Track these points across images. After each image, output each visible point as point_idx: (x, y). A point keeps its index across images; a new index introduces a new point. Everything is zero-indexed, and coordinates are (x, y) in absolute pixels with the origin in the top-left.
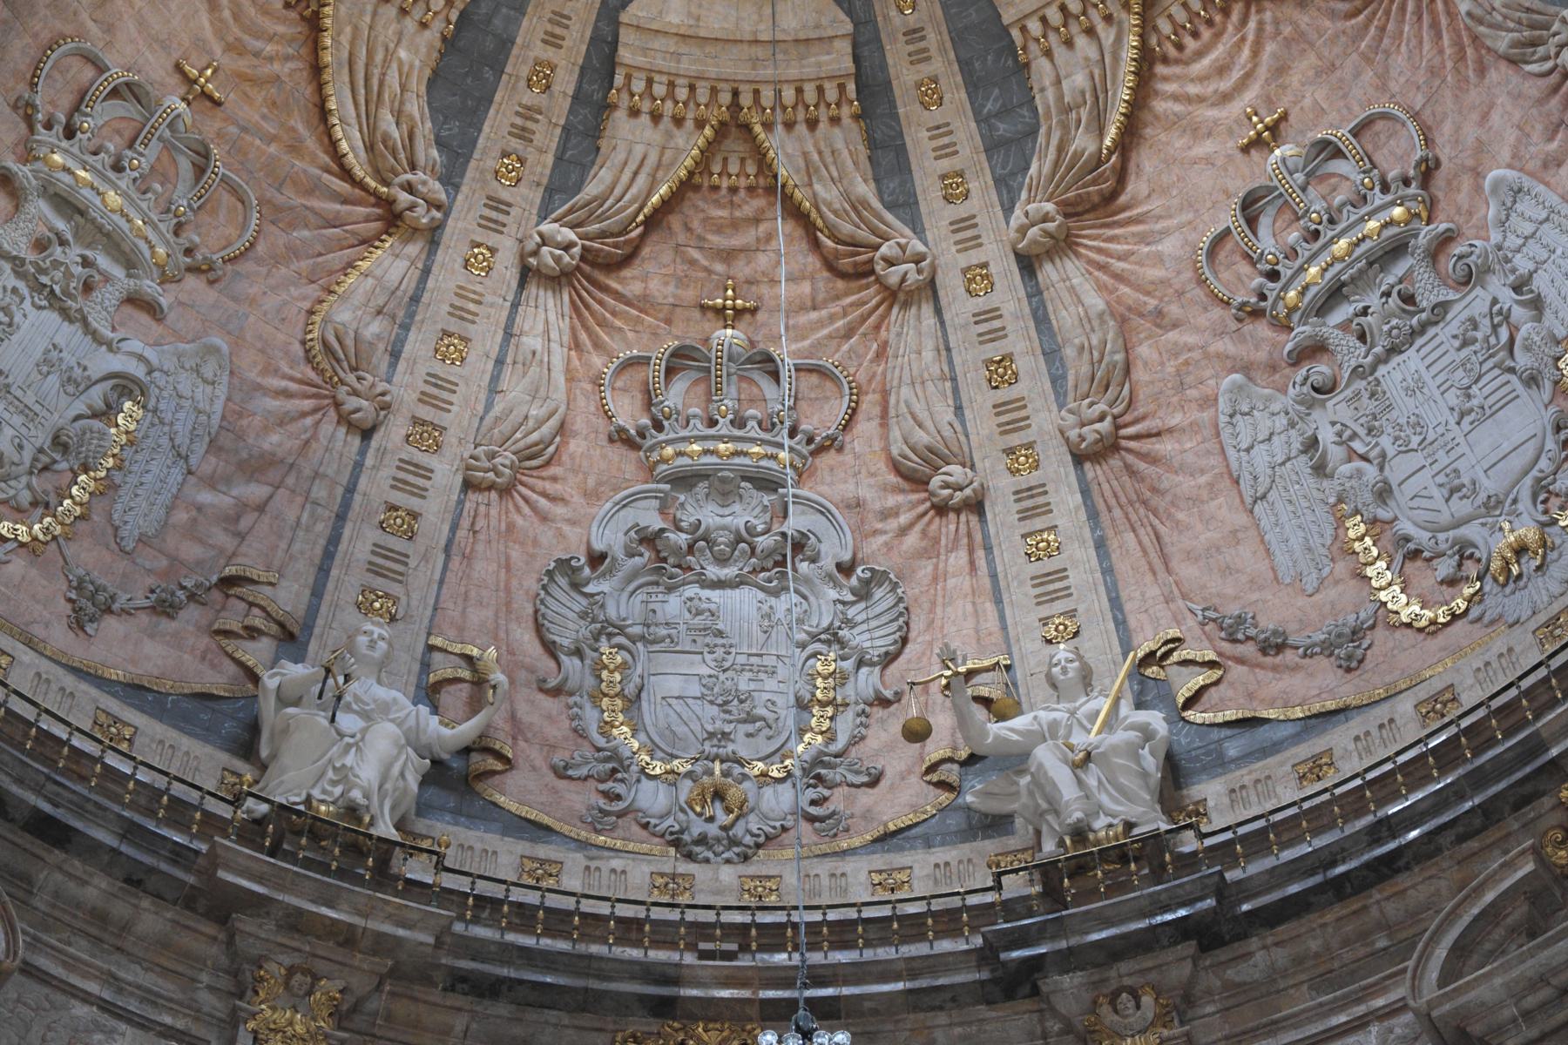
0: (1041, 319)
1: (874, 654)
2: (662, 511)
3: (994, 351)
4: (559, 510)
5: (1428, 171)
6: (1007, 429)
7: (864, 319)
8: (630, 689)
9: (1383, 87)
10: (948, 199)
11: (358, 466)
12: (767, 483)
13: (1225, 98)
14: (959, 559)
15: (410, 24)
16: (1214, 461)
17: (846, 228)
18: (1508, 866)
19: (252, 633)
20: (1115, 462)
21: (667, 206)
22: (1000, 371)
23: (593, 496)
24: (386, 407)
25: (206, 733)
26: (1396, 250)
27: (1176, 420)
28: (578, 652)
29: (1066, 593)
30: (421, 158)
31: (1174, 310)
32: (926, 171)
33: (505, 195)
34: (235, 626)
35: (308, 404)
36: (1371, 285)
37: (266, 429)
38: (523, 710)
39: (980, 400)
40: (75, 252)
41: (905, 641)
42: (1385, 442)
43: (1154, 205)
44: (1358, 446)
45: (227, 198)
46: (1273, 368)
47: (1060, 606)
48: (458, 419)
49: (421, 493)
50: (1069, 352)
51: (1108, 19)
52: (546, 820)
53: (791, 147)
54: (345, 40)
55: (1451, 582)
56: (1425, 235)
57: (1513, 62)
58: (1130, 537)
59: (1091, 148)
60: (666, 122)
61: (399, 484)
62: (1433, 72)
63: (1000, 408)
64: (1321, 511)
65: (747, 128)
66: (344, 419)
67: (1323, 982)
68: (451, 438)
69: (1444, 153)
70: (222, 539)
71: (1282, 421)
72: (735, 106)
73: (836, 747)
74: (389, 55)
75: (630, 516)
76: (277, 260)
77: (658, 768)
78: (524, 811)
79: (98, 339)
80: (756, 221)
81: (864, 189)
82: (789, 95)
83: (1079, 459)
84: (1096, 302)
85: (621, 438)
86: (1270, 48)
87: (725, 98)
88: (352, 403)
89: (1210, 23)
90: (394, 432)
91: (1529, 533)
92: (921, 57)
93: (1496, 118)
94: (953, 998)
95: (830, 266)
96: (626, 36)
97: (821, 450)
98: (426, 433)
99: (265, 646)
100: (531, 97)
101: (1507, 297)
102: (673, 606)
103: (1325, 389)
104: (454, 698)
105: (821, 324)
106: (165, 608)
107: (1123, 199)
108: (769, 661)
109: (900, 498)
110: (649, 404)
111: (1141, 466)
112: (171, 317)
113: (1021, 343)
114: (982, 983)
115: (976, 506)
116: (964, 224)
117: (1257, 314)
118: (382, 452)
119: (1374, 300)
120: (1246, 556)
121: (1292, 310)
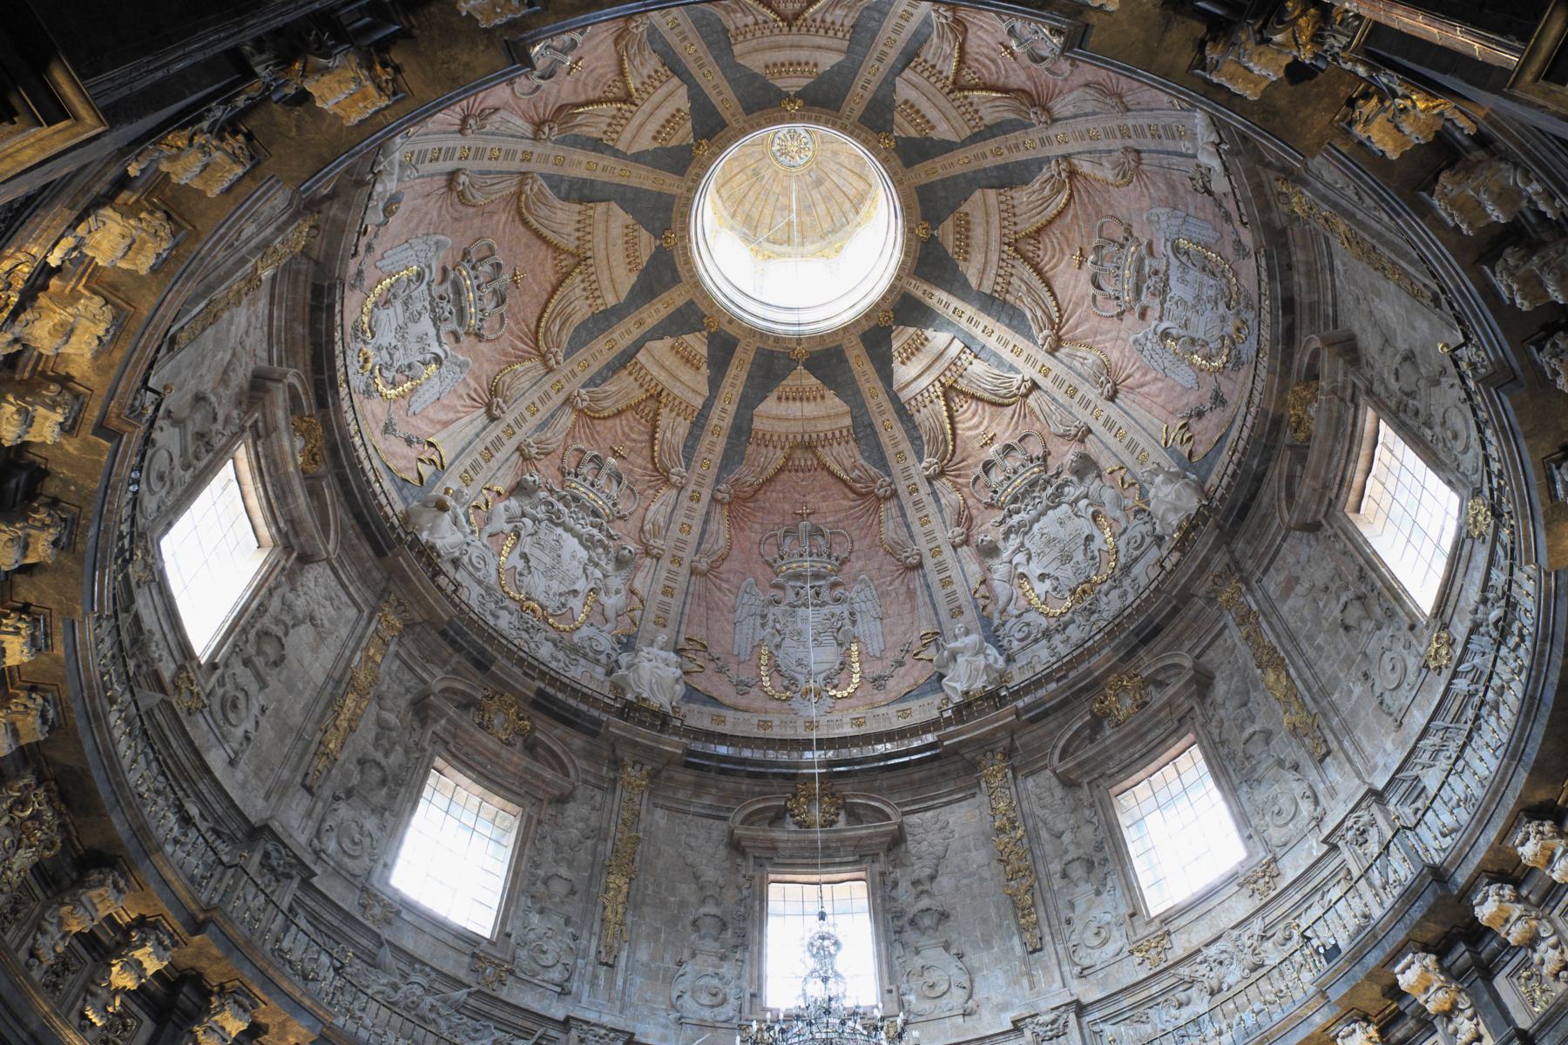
11: (1150, 151)
21: (997, 91)
45: (1105, 234)
53: (945, 68)
65: (954, 83)
72: (951, 91)
76: (1111, 206)
82: (933, 79)
88: (1133, 164)
90: (1131, 143)
95: (966, 30)
96: (963, 136)
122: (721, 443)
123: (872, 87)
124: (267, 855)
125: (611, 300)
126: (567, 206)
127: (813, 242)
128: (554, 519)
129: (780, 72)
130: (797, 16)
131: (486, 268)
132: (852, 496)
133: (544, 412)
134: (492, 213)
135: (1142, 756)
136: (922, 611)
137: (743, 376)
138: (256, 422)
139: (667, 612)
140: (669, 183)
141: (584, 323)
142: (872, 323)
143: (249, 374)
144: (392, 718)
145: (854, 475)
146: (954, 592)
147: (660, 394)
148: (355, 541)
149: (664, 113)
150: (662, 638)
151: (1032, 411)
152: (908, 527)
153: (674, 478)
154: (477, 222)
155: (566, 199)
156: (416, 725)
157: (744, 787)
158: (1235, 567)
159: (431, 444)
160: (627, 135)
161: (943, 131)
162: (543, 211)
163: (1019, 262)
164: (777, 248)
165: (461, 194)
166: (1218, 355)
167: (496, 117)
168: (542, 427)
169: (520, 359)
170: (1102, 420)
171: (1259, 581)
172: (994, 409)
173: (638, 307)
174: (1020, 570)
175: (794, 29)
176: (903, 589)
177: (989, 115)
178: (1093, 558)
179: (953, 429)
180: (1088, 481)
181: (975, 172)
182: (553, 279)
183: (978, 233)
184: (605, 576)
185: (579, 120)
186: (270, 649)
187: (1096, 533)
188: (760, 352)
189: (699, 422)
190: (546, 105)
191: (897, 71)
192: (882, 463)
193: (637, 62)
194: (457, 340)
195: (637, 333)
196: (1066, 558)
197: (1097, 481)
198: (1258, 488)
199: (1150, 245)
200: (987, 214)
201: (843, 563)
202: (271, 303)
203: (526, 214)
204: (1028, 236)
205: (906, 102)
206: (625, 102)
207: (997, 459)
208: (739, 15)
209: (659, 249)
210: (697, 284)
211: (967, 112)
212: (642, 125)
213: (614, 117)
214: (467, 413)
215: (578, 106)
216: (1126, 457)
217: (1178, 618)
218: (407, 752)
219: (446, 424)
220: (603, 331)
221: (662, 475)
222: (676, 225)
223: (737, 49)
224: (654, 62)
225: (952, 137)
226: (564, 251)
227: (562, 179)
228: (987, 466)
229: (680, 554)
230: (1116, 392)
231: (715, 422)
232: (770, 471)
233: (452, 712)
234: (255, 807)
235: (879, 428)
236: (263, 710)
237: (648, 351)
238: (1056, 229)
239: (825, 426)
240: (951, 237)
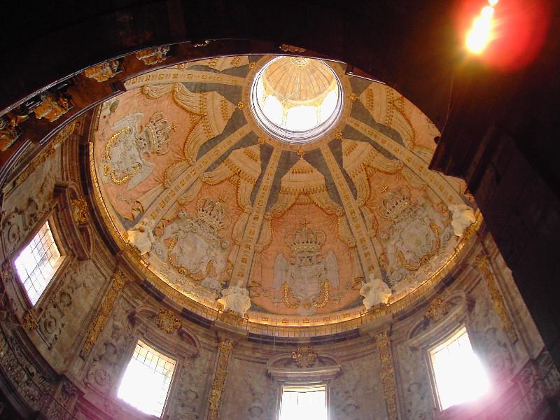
122: (268, 193)
124: (64, 387)
125: (216, 133)
126: (194, 94)
127: (311, 99)
128: (193, 231)
131: (160, 124)
133: (187, 184)
135: (445, 338)
138: (57, 204)
139: (244, 270)
140: (240, 81)
143: (53, 186)
144: (118, 324)
145: (326, 206)
147: (239, 173)
148: (103, 249)
150: (240, 282)
151: (404, 177)
153: (246, 210)
155: (194, 92)
156: (130, 326)
157: (274, 349)
159: (138, 202)
162: (184, 98)
164: (294, 102)
168: (187, 190)
171: (495, 259)
173: (229, 135)
176: (347, 258)
182: (190, 126)
183: (376, 98)
184: (216, 255)
186: (66, 300)
188: (283, 152)
189: (257, 185)
194: (148, 156)
195: (228, 147)
196: (418, 243)
201: (322, 245)
202: (62, 155)
210: (254, 123)
214: (154, 187)
217: (461, 275)
218: (126, 338)
219: (144, 193)
221: (241, 209)
222: (243, 99)
227: (192, 84)
229: (250, 244)
232: (290, 205)
233: (145, 320)
234: (59, 366)
235: (337, 184)
236: (63, 325)
239: (313, 184)
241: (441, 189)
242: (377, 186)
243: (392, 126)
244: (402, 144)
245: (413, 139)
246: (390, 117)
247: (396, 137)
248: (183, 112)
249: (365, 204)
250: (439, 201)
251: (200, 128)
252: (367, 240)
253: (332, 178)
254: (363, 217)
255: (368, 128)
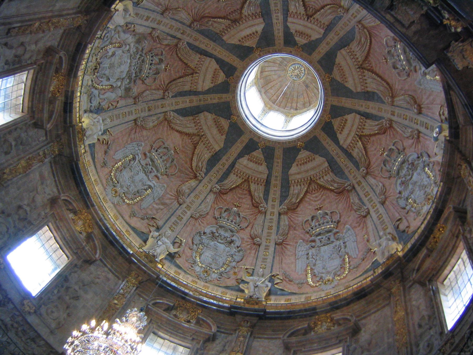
0: (279, 223)
1: (236, 260)
2: (216, 230)
3: (270, 225)
4: (202, 225)
5: (338, 222)
6: (268, 236)
7: (255, 213)
8: (201, 253)
9: (337, 208)
10: (272, 201)
11: (177, 209)
12: (232, 231)
13: (315, 201)
14: (254, 252)
15: (208, 152)
16: (294, 251)
17: (257, 200)
18: (304, 324)
19: (153, 226)
20: (281, 246)
21: (234, 188)
22: (270, 228)
23: (208, 224)
24: (184, 202)
25: (141, 237)
26: (330, 231)
27: (291, 243)
28: (196, 245)
29: (266, 262)
30: (203, 170)
31: (297, 228)
32: (271, 196)
33: (212, 179)
34: (151, 224)
35: (174, 198)
36: (325, 235)
37: (167, 199)
38: (185, 250)
39: (266, 231)
40: (151, 167)
41: (242, 260)
42: (318, 258)
43: (300, 213)
44: (314, 257)
45: (174, 167)
46: (307, 241)
47: (264, 263)
48: (194, 207)
49: (184, 215)
50: (281, 228)
51: (304, 184)
52: (181, 266)
54: (199, 151)
55: (318, 281)
56: (335, 230)
57: (356, 211)
58: (278, 258)
59: (294, 201)
60: (238, 177)
61: (182, 213)
62: (345, 208)
63: (268, 233)
64: (305, 264)
65: (249, 181)
66: (178, 202)
67: (274, 331)
68: (192, 209)
69: (342, 220)
70: (155, 212)
71: (305, 249)
72: (248, 178)
73: (226, 271)
74: (204, 155)
75: (211, 229)
77: (200, 265)
78: (179, 264)
79: (149, 179)
80: (245, 194)
81: (262, 195)
82: (256, 179)
83: (276, 244)
84: (287, 223)
85: (215, 218)
86: (324, 197)
87: (247, 176)
88: (180, 200)
89: (317, 190)
90: (184, 206)
91: (331, 278)
92: (276, 180)
93: (350, 218)
94: (223, 312)
95: (253, 204)
97: (242, 229)
98: (188, 207)
99: (154, 228)
100: (221, 167)
101: (342, 244)
102: (212, 243)
103: (313, 247)
104: (177, 245)
105: (248, 212)
106: (143, 219)
107: (296, 210)
108: (222, 256)
109: (250, 240)
110: (220, 214)
111: (284, 248)
112: (160, 180)
113: (274, 225)
114: (228, 312)
115: (259, 245)
116: (273, 205)
117: (308, 233)
118: (182, 208)
119: (324, 237)
120: (293, 266)
121: (313, 234)
122: (272, 7)
123: (275, 164)
125: (343, 52)
129: (309, 158)
130: (310, 184)
132: (207, 15)
134: (402, 89)
135: (34, 89)
136: (150, 5)
137: (276, 33)
141: (352, 40)
142: (235, 75)
145: (210, 23)
146: (142, 19)
147: (308, 19)
149: (346, 131)
151: (158, 89)
152: (177, 20)
154: (406, 87)
155: (374, 93)
158: (60, 154)
160: (357, 121)
161: (244, 161)
163: (196, 132)
165: (415, 102)
166: (115, 175)
167: (408, 134)
169: (374, 27)
170: (133, 111)
172: (172, 79)
173: (331, 49)
174: (124, 46)
175: (309, 178)
176: (163, 4)
177: (232, 177)
178: (102, 78)
179: (183, 62)
180: (123, 92)
181: (227, 152)
182: (370, 59)
183: (215, 131)
185: (376, 128)
187: (108, 83)
188: (274, 45)
189: (286, 12)
190: (390, 135)
191: (269, 176)
192: (202, 32)
193: (360, 155)
195: (328, 39)
197: (120, 95)
198: (75, 181)
199: (158, 178)
200: (215, 140)
203: (388, 87)
204: (198, 143)
205: (261, 164)
206: (361, 135)
207: (159, 66)
208: (329, 180)
209: (331, 74)
211: (240, 173)
212: (352, 126)
213: (364, 129)
215: (378, 134)
216: (116, 112)
220: (342, 38)
223: (326, 164)
224: (355, 154)
225: (241, 160)
226: (369, 70)
228: (161, 61)
230: (136, 124)
231: (279, 14)
232: (246, 6)
237: (320, 33)
238: (190, 153)
239: (232, 32)
240: (223, 123)
241: (125, 115)
242: (176, 64)
243: (191, 118)
244: (176, 111)
245: (169, 122)
246: (196, 124)
247: (184, 113)
248: (381, 74)
249: (176, 45)
250: (119, 105)
251: (360, 56)
252: (155, 26)
253: (219, 45)
254: (172, 36)
255: (210, 101)
